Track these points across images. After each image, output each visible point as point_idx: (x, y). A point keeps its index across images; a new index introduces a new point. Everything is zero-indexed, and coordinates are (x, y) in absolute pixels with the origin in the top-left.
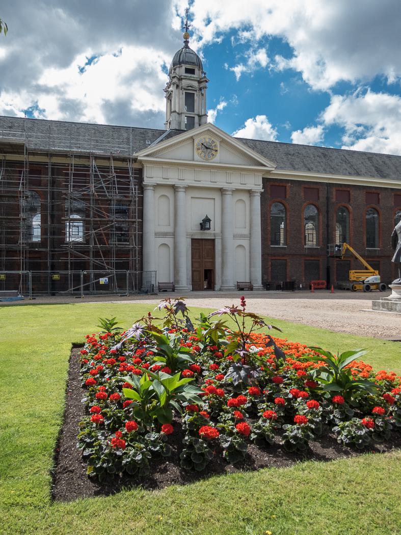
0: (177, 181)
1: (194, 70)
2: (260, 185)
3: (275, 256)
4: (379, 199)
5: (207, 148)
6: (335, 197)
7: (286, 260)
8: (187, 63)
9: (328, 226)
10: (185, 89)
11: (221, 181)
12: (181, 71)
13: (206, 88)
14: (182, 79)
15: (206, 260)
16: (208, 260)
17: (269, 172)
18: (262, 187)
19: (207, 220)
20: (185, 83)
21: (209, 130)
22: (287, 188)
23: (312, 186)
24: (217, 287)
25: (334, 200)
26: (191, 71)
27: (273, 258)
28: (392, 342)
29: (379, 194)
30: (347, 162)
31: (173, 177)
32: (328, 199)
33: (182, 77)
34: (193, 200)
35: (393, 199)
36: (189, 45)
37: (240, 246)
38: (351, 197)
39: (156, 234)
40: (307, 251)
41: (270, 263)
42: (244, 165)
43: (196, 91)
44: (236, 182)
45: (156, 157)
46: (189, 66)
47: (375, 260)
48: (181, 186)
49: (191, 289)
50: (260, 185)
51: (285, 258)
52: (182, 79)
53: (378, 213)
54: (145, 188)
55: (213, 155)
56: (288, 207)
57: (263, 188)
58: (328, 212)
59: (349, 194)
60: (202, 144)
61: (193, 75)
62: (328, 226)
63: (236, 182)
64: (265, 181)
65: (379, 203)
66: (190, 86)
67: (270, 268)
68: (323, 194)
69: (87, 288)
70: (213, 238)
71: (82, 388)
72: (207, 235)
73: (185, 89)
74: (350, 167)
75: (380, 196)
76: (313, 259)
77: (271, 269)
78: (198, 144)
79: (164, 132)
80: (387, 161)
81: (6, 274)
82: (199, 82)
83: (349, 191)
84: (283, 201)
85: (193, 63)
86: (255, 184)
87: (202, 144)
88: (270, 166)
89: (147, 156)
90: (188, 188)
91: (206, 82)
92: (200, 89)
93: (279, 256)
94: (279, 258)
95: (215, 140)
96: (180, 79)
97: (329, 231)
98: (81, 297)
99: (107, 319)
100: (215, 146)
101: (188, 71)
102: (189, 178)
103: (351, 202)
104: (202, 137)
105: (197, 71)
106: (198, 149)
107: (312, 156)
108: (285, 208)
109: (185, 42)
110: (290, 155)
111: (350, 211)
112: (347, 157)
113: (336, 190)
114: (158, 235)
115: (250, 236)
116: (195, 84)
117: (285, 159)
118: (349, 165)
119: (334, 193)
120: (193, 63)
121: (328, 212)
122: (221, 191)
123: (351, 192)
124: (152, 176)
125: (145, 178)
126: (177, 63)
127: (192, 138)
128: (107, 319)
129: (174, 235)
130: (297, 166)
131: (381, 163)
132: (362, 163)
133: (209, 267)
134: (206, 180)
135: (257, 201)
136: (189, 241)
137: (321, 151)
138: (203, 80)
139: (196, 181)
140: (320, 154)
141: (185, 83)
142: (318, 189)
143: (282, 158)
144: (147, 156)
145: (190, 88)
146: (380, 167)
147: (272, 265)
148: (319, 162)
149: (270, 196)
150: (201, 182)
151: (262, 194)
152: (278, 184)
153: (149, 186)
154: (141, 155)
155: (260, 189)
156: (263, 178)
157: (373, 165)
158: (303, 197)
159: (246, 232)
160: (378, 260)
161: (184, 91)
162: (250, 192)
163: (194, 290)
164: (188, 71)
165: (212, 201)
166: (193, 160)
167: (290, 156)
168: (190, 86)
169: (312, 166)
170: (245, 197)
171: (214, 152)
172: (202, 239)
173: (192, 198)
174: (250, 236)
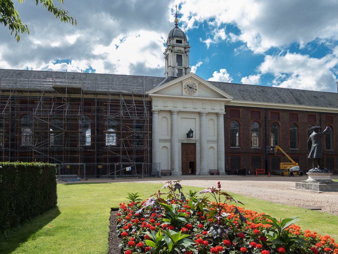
0: (173, 108)
1: (182, 41)
2: (223, 110)
4: (298, 118)
5: (190, 88)
6: (270, 117)
7: (240, 156)
8: (177, 37)
9: (266, 134)
11: (199, 108)
12: (174, 42)
13: (189, 51)
14: (174, 46)
15: (190, 156)
16: (192, 156)
17: (228, 102)
18: (224, 111)
19: (191, 132)
20: (176, 49)
21: (191, 77)
22: (240, 111)
23: (256, 110)
24: (197, 173)
25: (269, 119)
26: (180, 42)
28: (311, 210)
29: (298, 115)
30: (277, 95)
31: (170, 106)
32: (265, 118)
33: (175, 45)
35: (307, 118)
38: (280, 117)
39: (160, 140)
40: (253, 150)
41: (230, 158)
42: (214, 98)
43: (183, 53)
44: (209, 108)
47: (296, 156)
48: (175, 111)
49: (181, 174)
50: (223, 110)
51: (239, 155)
52: (174, 46)
53: (298, 127)
54: (153, 113)
55: (194, 92)
56: (241, 123)
57: (225, 112)
58: (266, 126)
59: (279, 115)
60: (188, 85)
61: (181, 44)
62: (266, 134)
64: (226, 107)
65: (298, 120)
66: (180, 51)
67: (230, 161)
68: (262, 115)
70: (194, 142)
71: (118, 237)
72: (191, 141)
74: (279, 98)
75: (298, 116)
76: (257, 155)
78: (185, 86)
79: (164, 78)
80: (303, 94)
82: (185, 48)
83: (279, 113)
84: (238, 120)
85: (181, 37)
86: (221, 109)
87: (188, 85)
88: (229, 98)
90: (179, 112)
91: (189, 48)
92: (186, 52)
94: (236, 155)
95: (195, 83)
96: (173, 47)
97: (267, 138)
98: (115, 179)
99: (132, 194)
100: (196, 86)
101: (178, 41)
102: (180, 106)
103: (280, 120)
104: (187, 81)
105: (183, 41)
106: (185, 89)
107: (255, 91)
108: (239, 124)
110: (242, 91)
111: (280, 125)
112: (277, 92)
113: (271, 112)
114: (161, 141)
115: (217, 141)
116: (183, 49)
117: (238, 94)
118: (278, 97)
119: (270, 114)
120: (181, 37)
121: (266, 126)
122: (200, 114)
123: (280, 113)
124: (157, 106)
125: (153, 107)
126: (171, 37)
127: (181, 82)
128: (132, 194)
129: (171, 141)
130: (246, 98)
131: (299, 95)
132: (287, 95)
133: (192, 160)
134: (190, 107)
135: (222, 119)
136: (180, 144)
137: (261, 88)
138: (187, 47)
140: (260, 90)
141: (176, 49)
142: (259, 112)
143: (237, 93)
145: (180, 52)
146: (298, 98)
148: (260, 95)
150: (187, 109)
151: (224, 115)
153: (155, 111)
154: (150, 93)
155: (223, 112)
156: (225, 105)
157: (294, 97)
158: (250, 116)
159: (215, 138)
160: (298, 156)
161: (176, 54)
162: (217, 114)
163: (183, 174)
164: (178, 41)
165: (194, 120)
166: (182, 95)
167: (241, 92)
169: (256, 97)
170: (214, 117)
171: (194, 90)
172: (188, 144)
173: (181, 118)
174: (217, 141)
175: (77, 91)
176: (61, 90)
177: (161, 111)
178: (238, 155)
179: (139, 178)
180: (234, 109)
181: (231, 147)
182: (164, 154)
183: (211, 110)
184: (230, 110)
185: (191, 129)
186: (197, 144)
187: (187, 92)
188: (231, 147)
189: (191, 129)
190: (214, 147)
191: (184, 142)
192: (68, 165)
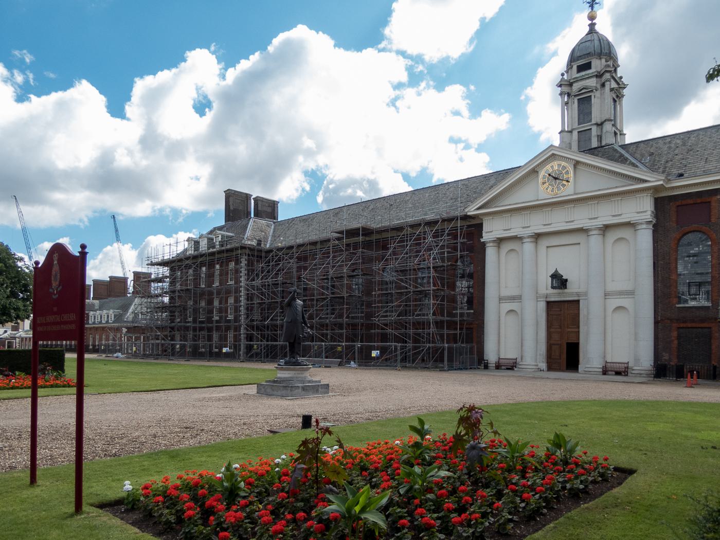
3: (685, 322)
5: (556, 178)
7: (710, 328)
10: (575, 96)
15: (569, 330)
17: (656, 189)
20: (576, 87)
26: (588, 66)
27: (682, 325)
34: (549, 249)
36: (597, 28)
37: (619, 308)
41: (675, 334)
43: (592, 91)
44: (606, 214)
45: (495, 207)
46: (581, 62)
63: (606, 214)
66: (584, 88)
67: (676, 342)
69: (404, 360)
72: (569, 294)
73: (575, 96)
77: (679, 344)
78: (544, 177)
81: (181, 344)
86: (642, 210)
87: (549, 175)
89: (479, 209)
93: (693, 321)
94: (694, 325)
96: (571, 85)
106: (544, 183)
109: (589, 25)
116: (592, 82)
124: (491, 230)
125: (484, 234)
133: (572, 340)
136: (542, 306)
139: (545, 225)
141: (576, 87)
144: (479, 209)
147: (679, 337)
149: (675, 225)
152: (692, 202)
153: (488, 242)
154: (472, 211)
163: (550, 368)
164: (581, 69)
165: (577, 246)
168: (584, 88)
171: (564, 182)
173: (547, 247)
175: (367, 232)
176: (352, 233)
177: (500, 241)
178: (702, 325)
179: (440, 371)
180: (690, 201)
181: (677, 306)
182: (512, 325)
183: (566, 224)
184: (678, 206)
185: (556, 271)
186: (581, 301)
187: (547, 189)
188: (677, 306)
189: (556, 271)
190: (626, 306)
191: (553, 299)
192: (339, 346)
